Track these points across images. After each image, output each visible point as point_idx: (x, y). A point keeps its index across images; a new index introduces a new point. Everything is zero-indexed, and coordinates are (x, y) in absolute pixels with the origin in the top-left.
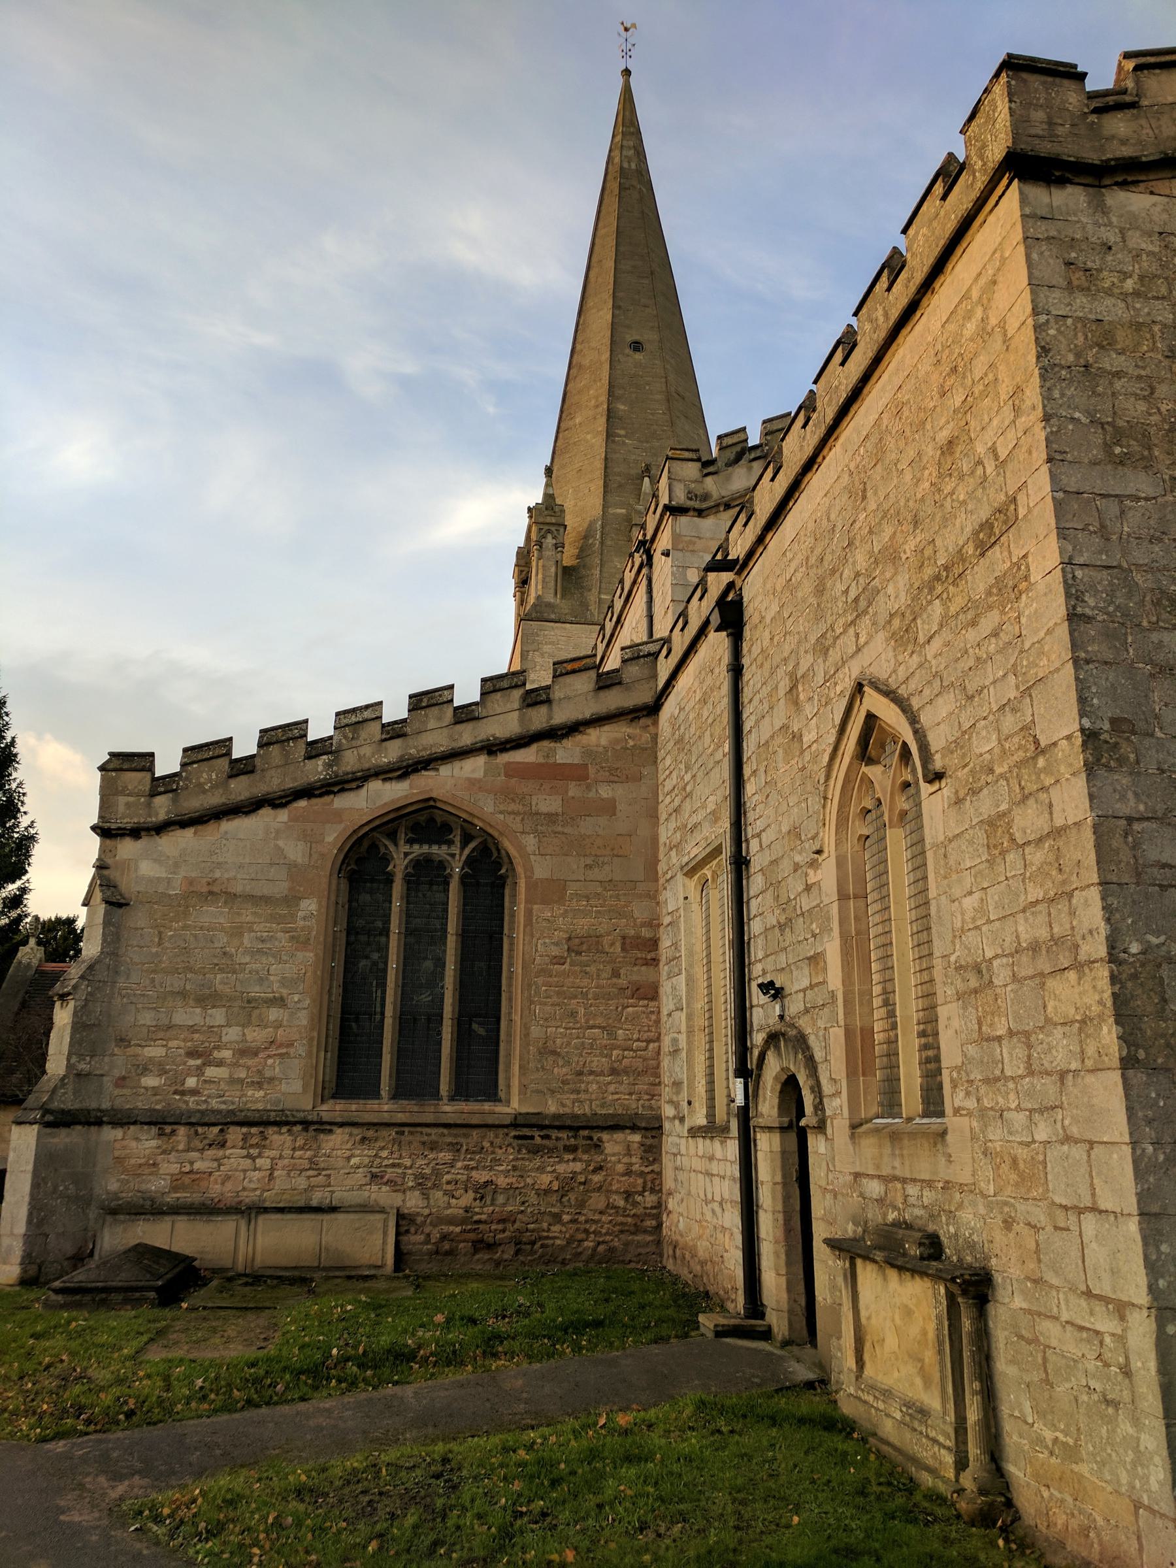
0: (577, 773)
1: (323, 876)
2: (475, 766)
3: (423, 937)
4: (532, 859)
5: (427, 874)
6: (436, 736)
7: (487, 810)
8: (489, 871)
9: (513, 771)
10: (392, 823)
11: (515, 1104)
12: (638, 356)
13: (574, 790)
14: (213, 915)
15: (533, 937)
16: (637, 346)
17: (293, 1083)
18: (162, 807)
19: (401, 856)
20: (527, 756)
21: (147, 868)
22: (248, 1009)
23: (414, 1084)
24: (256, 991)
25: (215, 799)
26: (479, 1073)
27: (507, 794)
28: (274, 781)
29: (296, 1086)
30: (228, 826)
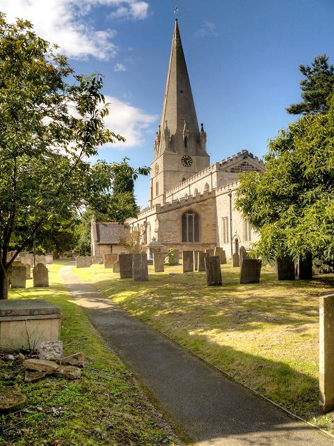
2: (195, 205)
3: (190, 225)
4: (203, 216)
6: (191, 201)
7: (197, 210)
8: (197, 217)
11: (202, 242)
14: (169, 222)
15: (203, 224)
16: (182, 92)
17: (179, 240)
18: (163, 210)
19: (188, 215)
20: (201, 203)
21: (162, 217)
26: (197, 239)
28: (174, 207)
30: (170, 212)
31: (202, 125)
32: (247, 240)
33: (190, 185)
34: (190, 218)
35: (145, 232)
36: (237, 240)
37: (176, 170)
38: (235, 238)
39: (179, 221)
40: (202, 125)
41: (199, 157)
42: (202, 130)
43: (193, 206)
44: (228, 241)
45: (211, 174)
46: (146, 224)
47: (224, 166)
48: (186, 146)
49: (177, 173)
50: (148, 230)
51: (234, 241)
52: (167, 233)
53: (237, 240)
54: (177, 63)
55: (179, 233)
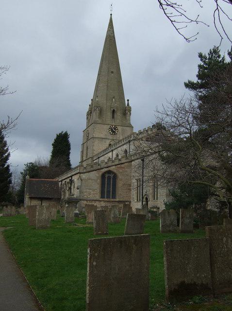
0: (123, 168)
1: (100, 178)
2: (114, 167)
3: (109, 184)
4: (120, 176)
5: (109, 178)
6: (110, 164)
7: (115, 171)
8: (115, 176)
9: (117, 167)
10: (105, 173)
12: (112, 74)
13: (123, 170)
15: (120, 184)
16: (112, 72)
17: (98, 197)
19: (107, 176)
20: (119, 166)
21: (84, 176)
22: (94, 190)
23: (108, 197)
24: (94, 188)
25: (89, 170)
26: (114, 197)
27: (116, 169)
28: (95, 168)
29: (98, 197)
31: (128, 100)
32: (154, 199)
33: (112, 151)
34: (109, 178)
35: (70, 188)
36: (147, 199)
37: (104, 137)
38: (145, 197)
39: (99, 181)
40: (128, 100)
41: (125, 128)
42: (128, 103)
43: (111, 169)
44: (140, 199)
45: (129, 142)
46: (71, 181)
47: (140, 136)
48: (113, 117)
49: (104, 140)
50: (72, 187)
51: (144, 200)
52: (88, 191)
53: (147, 199)
54: (106, 39)
55: (98, 191)
